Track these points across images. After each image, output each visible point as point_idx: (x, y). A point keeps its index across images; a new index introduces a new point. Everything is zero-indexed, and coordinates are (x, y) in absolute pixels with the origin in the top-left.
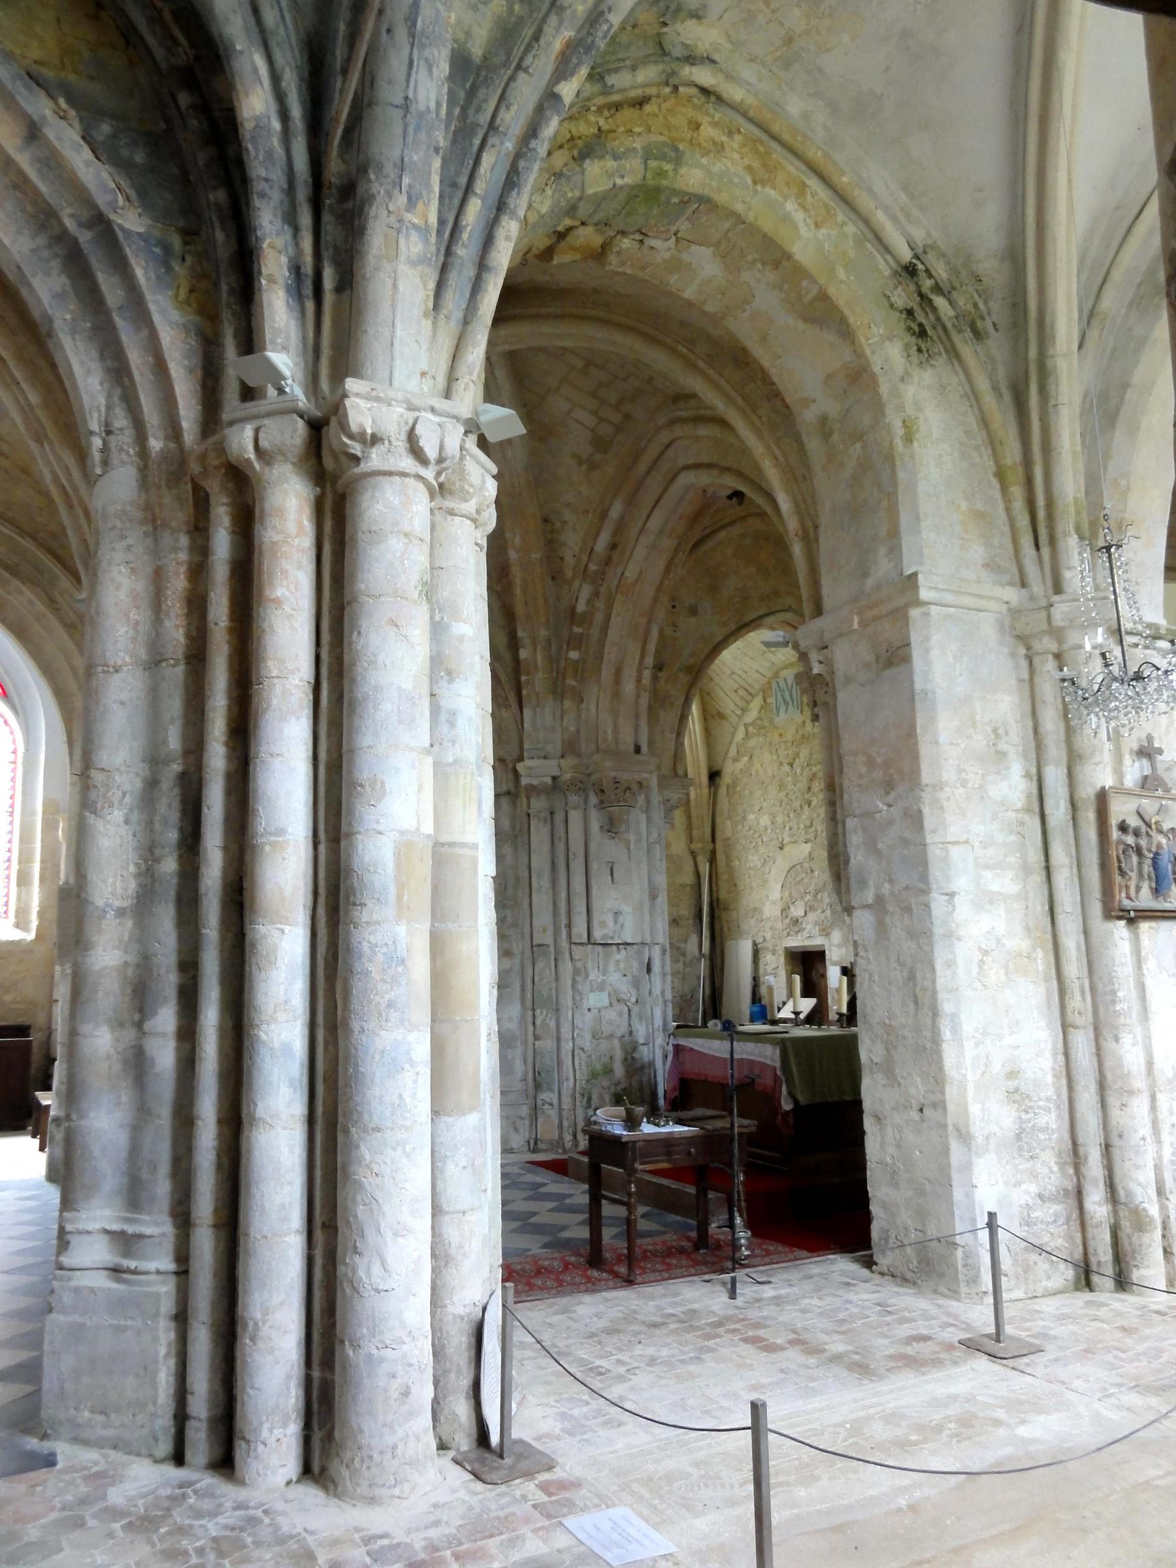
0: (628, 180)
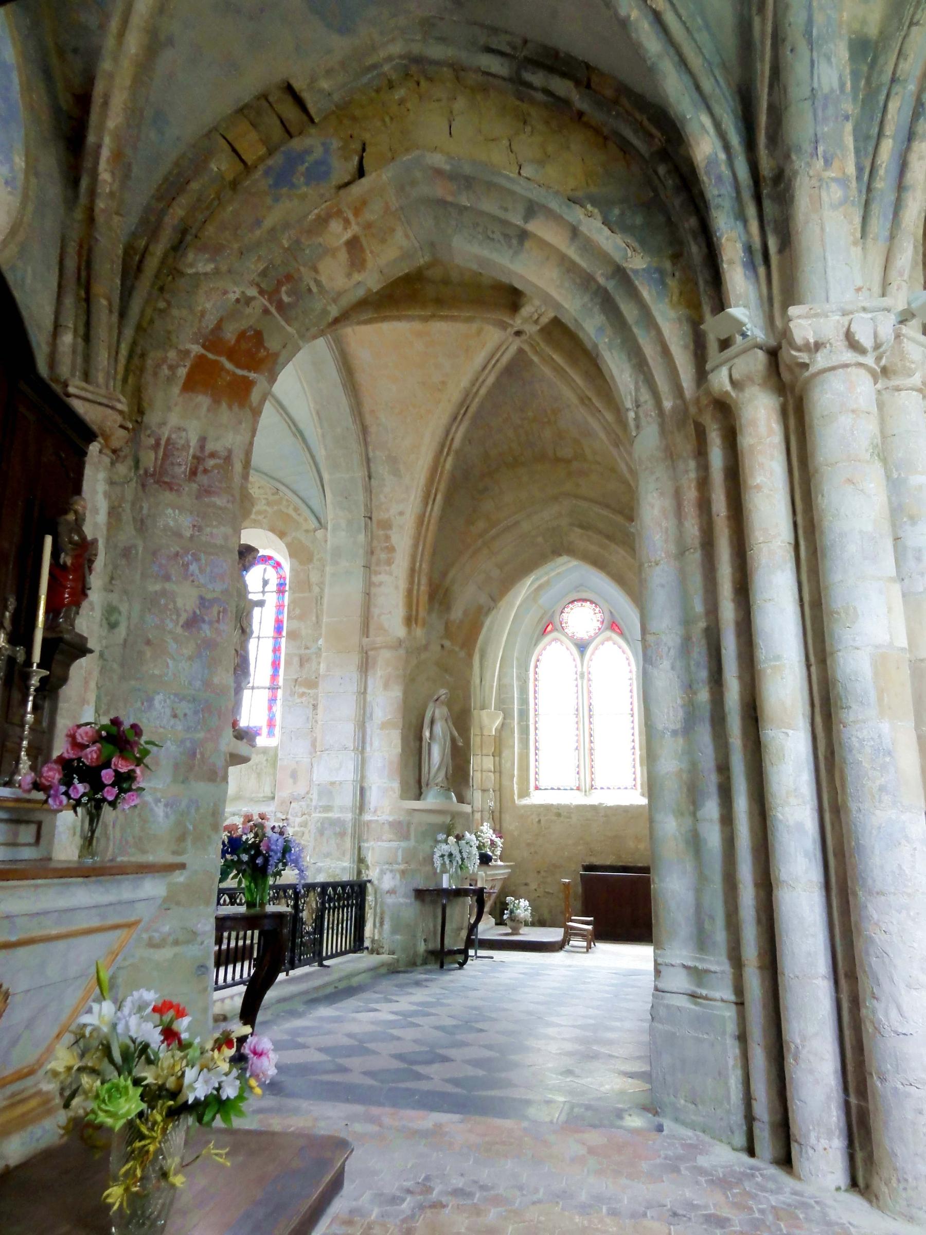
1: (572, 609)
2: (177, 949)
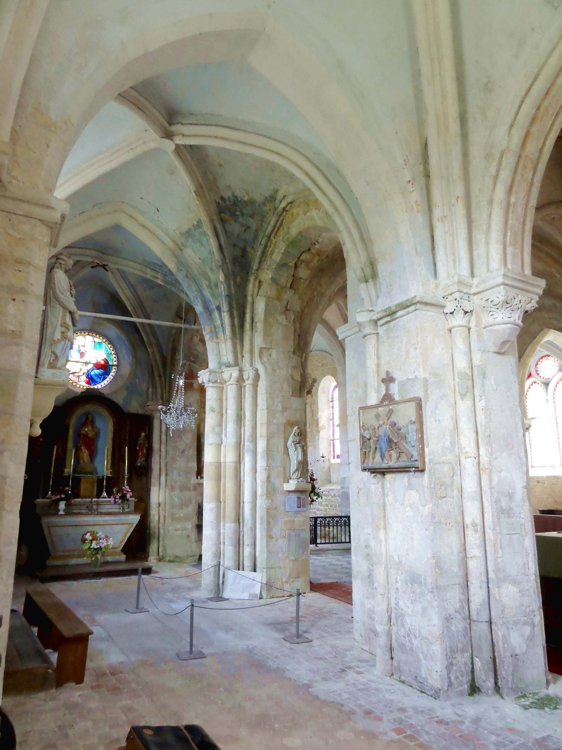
0: (283, 249)
1: (542, 362)
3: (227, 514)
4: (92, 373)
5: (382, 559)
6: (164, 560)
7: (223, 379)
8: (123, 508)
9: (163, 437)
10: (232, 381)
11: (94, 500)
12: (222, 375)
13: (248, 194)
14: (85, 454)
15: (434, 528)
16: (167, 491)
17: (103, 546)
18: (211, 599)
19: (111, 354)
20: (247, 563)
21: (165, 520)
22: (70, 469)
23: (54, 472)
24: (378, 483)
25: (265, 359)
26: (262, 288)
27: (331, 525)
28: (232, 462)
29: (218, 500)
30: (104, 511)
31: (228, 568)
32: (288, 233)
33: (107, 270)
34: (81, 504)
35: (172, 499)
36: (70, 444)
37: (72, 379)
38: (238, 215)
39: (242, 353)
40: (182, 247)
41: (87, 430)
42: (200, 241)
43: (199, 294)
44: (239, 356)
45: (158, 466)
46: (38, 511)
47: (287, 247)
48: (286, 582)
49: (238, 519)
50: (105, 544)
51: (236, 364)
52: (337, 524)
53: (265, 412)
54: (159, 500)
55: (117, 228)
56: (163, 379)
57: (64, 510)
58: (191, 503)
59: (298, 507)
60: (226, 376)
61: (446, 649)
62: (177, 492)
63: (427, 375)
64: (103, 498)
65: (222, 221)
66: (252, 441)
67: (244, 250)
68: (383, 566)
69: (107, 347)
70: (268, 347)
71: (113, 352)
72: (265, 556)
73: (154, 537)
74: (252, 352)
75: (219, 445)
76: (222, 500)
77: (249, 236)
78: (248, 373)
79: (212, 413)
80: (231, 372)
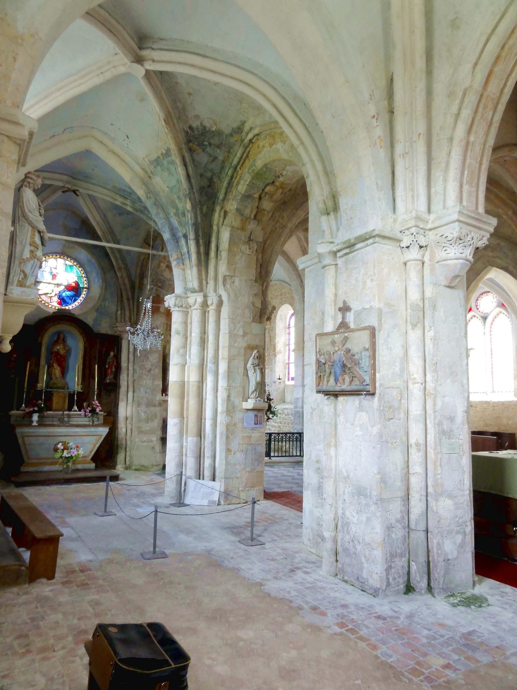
0: (249, 180)
1: (482, 298)
2: (148, 443)
3: (189, 429)
4: (64, 294)
5: (332, 473)
6: (131, 468)
7: (188, 304)
8: (93, 421)
9: (131, 356)
10: (197, 306)
11: (65, 413)
12: (187, 301)
13: (216, 125)
14: (57, 371)
15: (381, 446)
16: (134, 406)
17: (73, 455)
18: (173, 505)
19: (82, 277)
20: (207, 473)
21: (132, 433)
22: (43, 383)
23: (27, 387)
24: (331, 404)
25: (228, 286)
26: (227, 218)
27: (284, 440)
28: (195, 381)
29: (181, 415)
30: (75, 423)
31: (190, 478)
32: (254, 165)
33: (77, 195)
34: (53, 417)
35: (138, 413)
36: (43, 361)
37: (44, 299)
38: (205, 145)
39: (206, 280)
40: (151, 175)
41: (59, 348)
42: (168, 170)
43: (167, 222)
44: (204, 282)
45: (126, 383)
46: (12, 421)
47: (252, 179)
48: (243, 491)
49: (200, 434)
50: (76, 453)
51: (201, 290)
52: (289, 439)
53: (227, 336)
54: (126, 415)
55: (88, 153)
56: (131, 302)
57: (37, 422)
58: (156, 418)
59: (255, 424)
60: (191, 301)
61: (386, 554)
62: (143, 408)
63: (381, 305)
64: (74, 411)
65: (191, 150)
66: (214, 363)
67: (211, 180)
68: (332, 480)
69: (78, 270)
70: (232, 275)
71: (84, 275)
72: (224, 467)
73: (122, 448)
74: (216, 280)
75: (183, 366)
76: (185, 416)
77: (215, 166)
78: (212, 299)
79: (177, 336)
80: (196, 297)
